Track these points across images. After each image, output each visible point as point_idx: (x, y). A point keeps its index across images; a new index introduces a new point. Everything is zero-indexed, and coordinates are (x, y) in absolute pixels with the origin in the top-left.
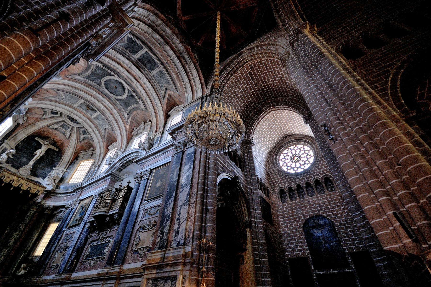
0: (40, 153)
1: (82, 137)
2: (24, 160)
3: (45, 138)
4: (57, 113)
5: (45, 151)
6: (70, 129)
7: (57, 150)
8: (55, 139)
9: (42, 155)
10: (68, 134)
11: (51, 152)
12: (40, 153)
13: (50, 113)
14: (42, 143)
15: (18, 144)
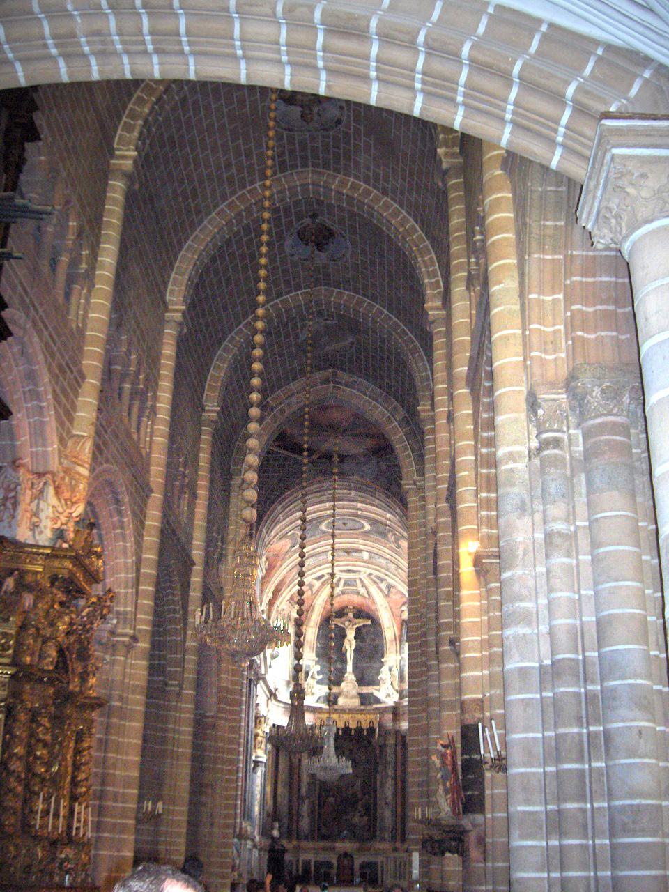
0: (350, 644)
1: (383, 585)
2: (339, 665)
3: (341, 613)
4: (322, 576)
5: (356, 638)
6: (358, 582)
7: (370, 623)
8: (355, 605)
9: (353, 647)
10: (362, 591)
11: (364, 631)
12: (350, 644)
13: (315, 581)
14: (342, 626)
15: (317, 647)
